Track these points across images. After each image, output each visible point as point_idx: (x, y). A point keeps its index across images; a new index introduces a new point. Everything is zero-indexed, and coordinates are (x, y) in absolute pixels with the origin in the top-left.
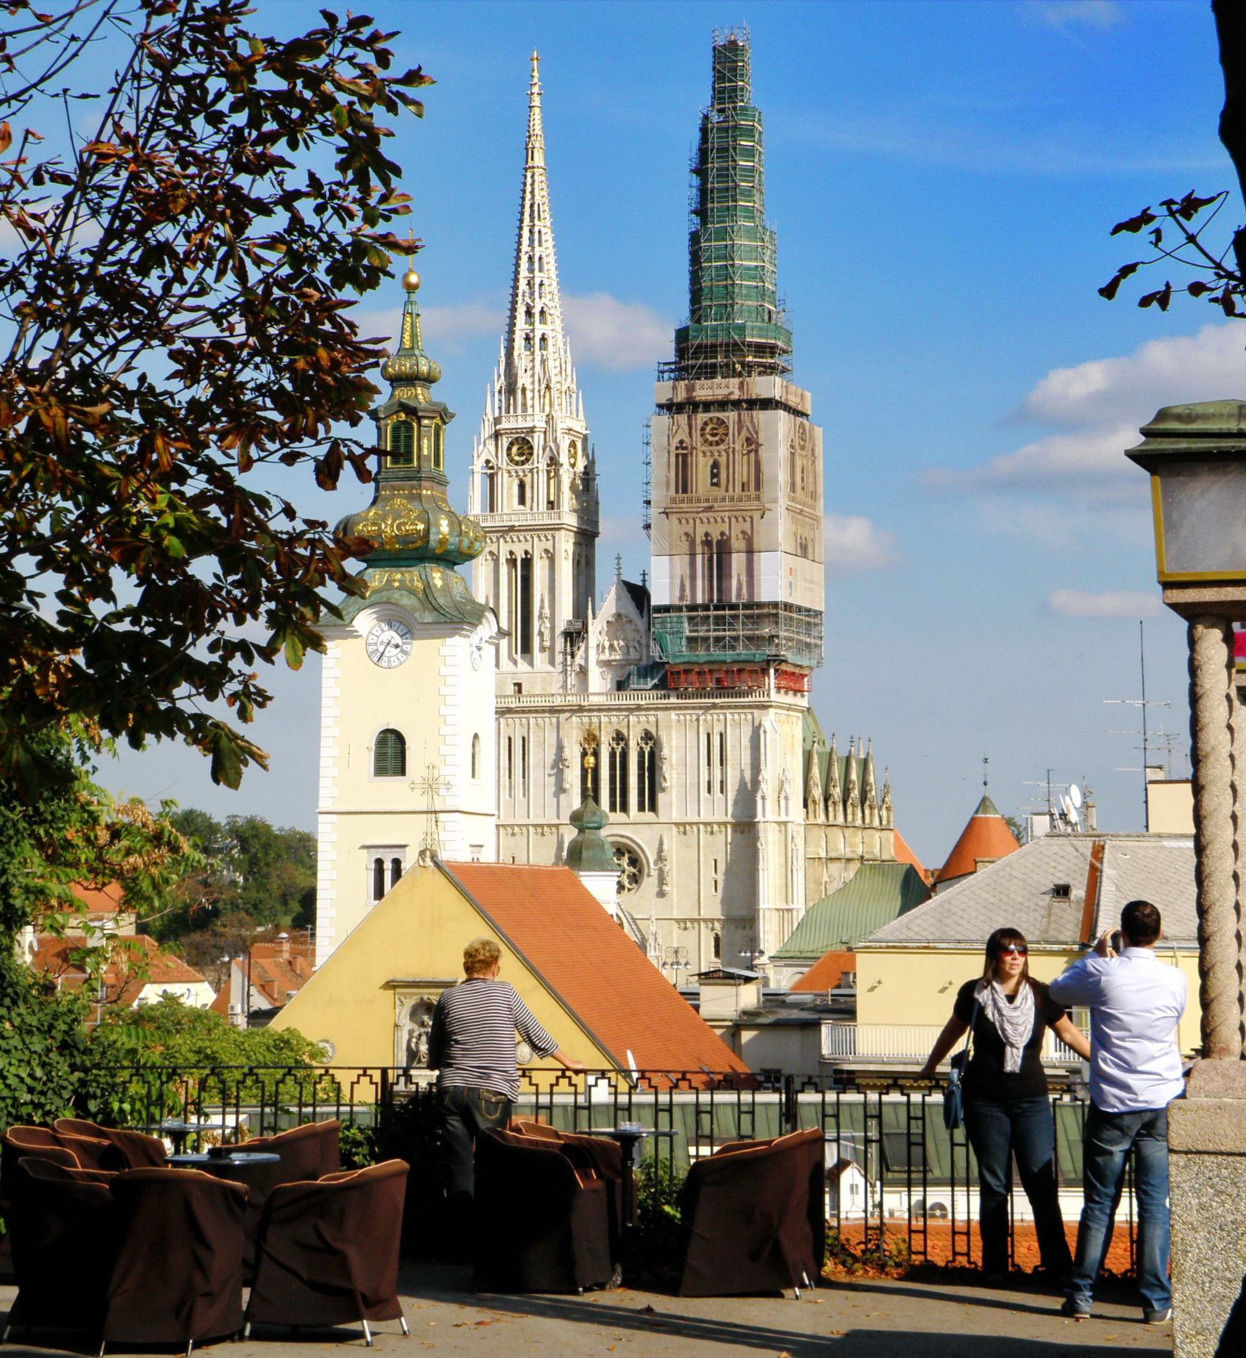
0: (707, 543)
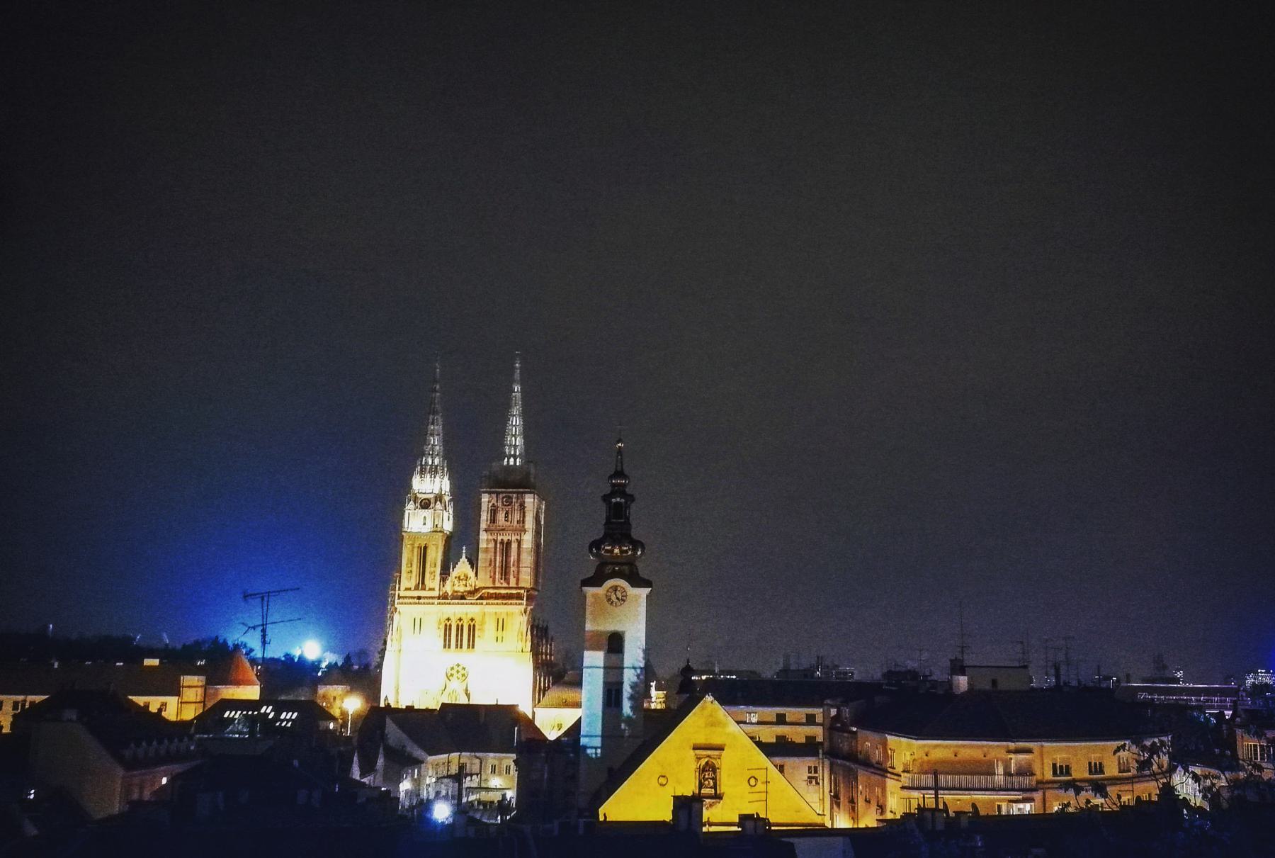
0: (502, 542)
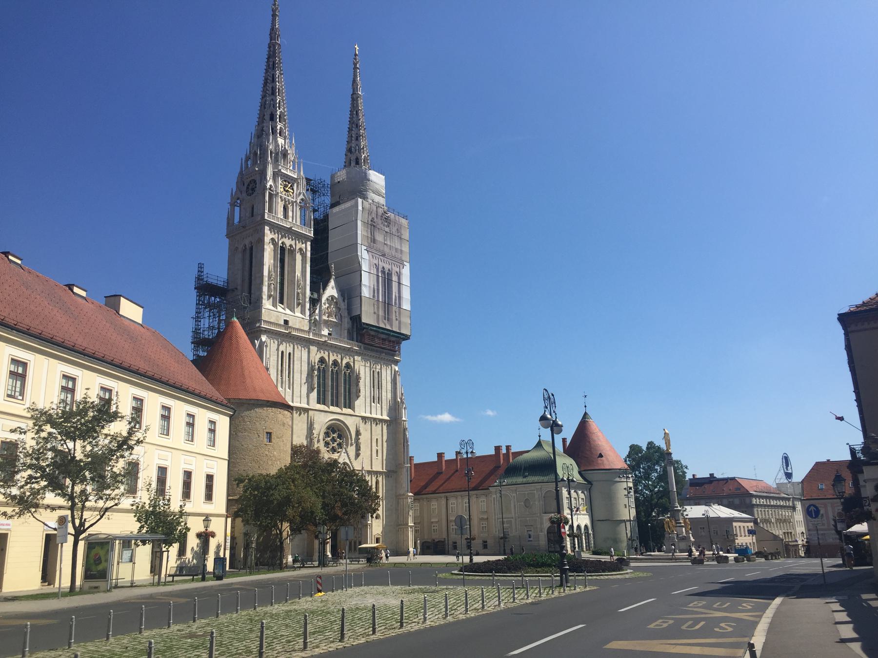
0: (383, 272)
